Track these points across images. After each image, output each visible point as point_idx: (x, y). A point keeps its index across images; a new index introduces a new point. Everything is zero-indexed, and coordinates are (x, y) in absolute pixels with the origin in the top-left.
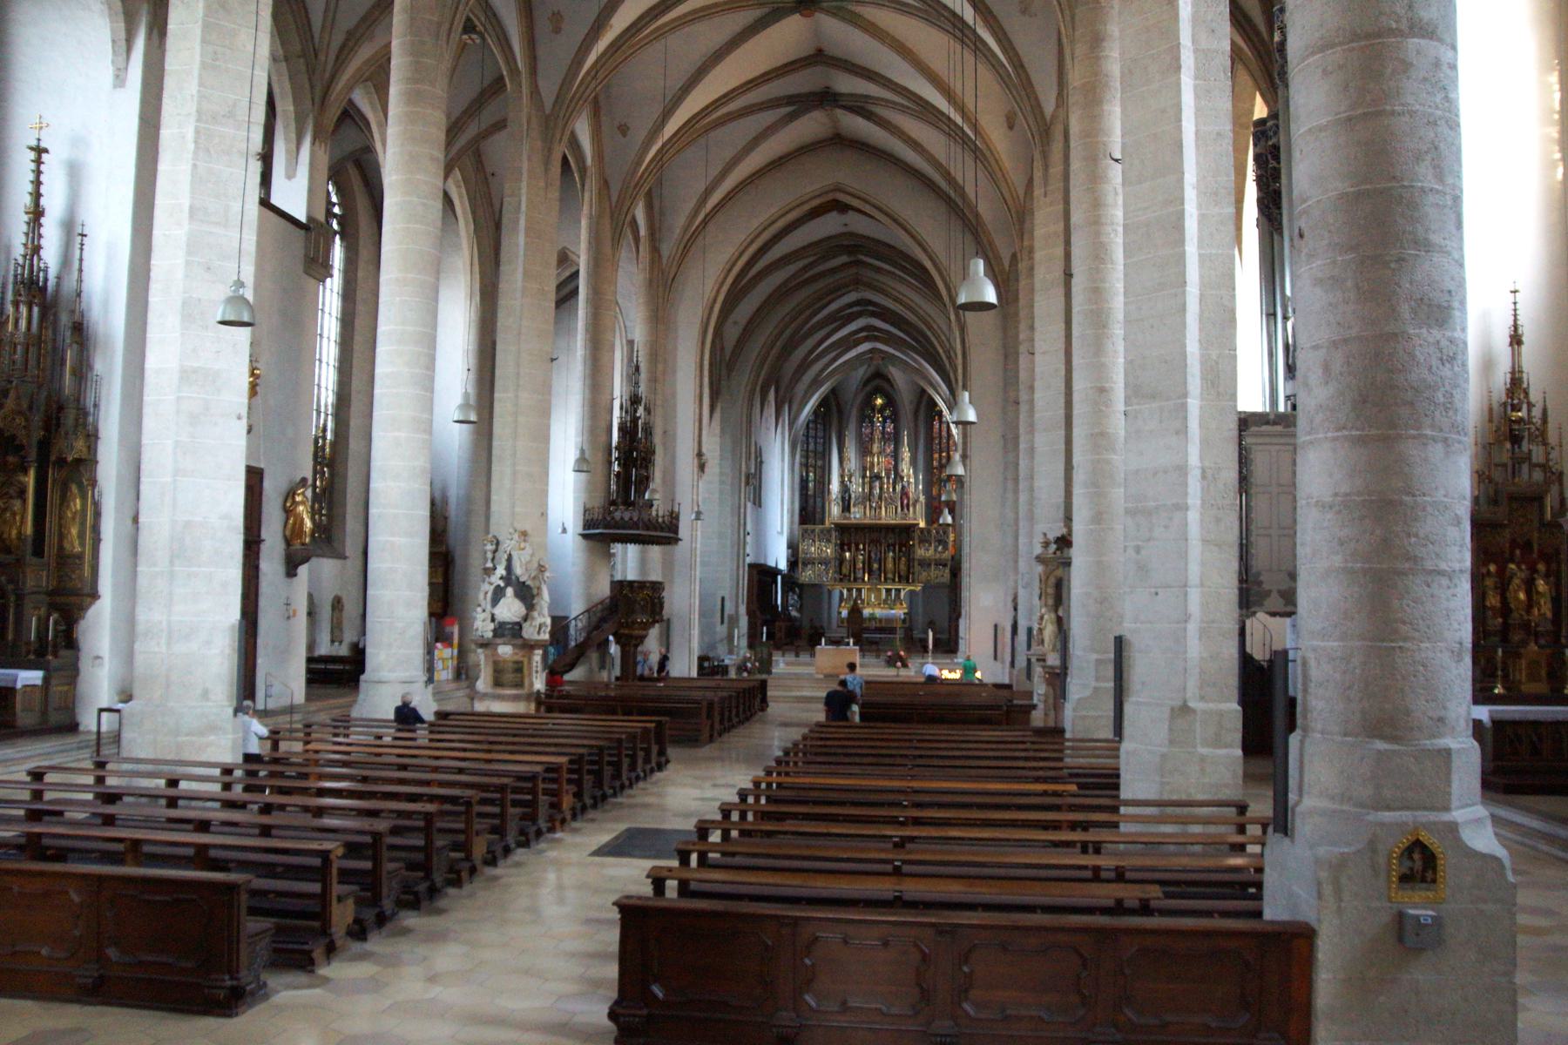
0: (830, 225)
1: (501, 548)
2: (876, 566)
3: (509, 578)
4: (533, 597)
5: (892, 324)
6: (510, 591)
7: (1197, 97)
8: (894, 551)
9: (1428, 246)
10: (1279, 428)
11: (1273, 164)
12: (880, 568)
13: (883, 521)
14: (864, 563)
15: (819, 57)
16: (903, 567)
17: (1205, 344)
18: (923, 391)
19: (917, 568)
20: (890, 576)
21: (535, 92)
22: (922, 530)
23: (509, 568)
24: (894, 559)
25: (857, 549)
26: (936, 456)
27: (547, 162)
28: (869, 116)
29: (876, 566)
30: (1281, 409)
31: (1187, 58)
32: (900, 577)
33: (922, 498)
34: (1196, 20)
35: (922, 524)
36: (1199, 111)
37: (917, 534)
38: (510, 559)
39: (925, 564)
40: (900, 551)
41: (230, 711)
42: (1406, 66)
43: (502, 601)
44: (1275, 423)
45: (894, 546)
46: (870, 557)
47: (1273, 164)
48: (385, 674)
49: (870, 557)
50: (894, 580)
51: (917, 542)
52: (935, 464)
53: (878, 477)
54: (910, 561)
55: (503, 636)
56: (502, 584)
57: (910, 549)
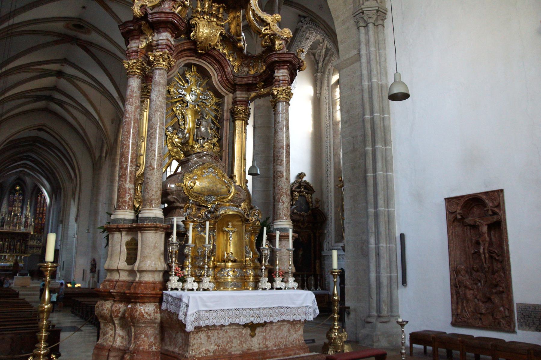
0: (34, 133)
2: (12, 247)
5: (35, 164)
8: (20, 242)
12: (14, 248)
13: (17, 231)
14: (7, 246)
15: (55, 88)
16: (23, 248)
18: (36, 186)
19: (29, 249)
20: (18, 251)
22: (32, 235)
24: (20, 245)
25: (5, 241)
26: (38, 209)
28: (62, 107)
29: (12, 247)
32: (21, 251)
33: (33, 224)
35: (32, 233)
37: (30, 236)
39: (32, 247)
40: (23, 242)
45: (20, 240)
46: (10, 244)
49: (10, 244)
50: (19, 252)
51: (29, 239)
52: (38, 212)
53: (16, 215)
54: (26, 246)
57: (27, 241)
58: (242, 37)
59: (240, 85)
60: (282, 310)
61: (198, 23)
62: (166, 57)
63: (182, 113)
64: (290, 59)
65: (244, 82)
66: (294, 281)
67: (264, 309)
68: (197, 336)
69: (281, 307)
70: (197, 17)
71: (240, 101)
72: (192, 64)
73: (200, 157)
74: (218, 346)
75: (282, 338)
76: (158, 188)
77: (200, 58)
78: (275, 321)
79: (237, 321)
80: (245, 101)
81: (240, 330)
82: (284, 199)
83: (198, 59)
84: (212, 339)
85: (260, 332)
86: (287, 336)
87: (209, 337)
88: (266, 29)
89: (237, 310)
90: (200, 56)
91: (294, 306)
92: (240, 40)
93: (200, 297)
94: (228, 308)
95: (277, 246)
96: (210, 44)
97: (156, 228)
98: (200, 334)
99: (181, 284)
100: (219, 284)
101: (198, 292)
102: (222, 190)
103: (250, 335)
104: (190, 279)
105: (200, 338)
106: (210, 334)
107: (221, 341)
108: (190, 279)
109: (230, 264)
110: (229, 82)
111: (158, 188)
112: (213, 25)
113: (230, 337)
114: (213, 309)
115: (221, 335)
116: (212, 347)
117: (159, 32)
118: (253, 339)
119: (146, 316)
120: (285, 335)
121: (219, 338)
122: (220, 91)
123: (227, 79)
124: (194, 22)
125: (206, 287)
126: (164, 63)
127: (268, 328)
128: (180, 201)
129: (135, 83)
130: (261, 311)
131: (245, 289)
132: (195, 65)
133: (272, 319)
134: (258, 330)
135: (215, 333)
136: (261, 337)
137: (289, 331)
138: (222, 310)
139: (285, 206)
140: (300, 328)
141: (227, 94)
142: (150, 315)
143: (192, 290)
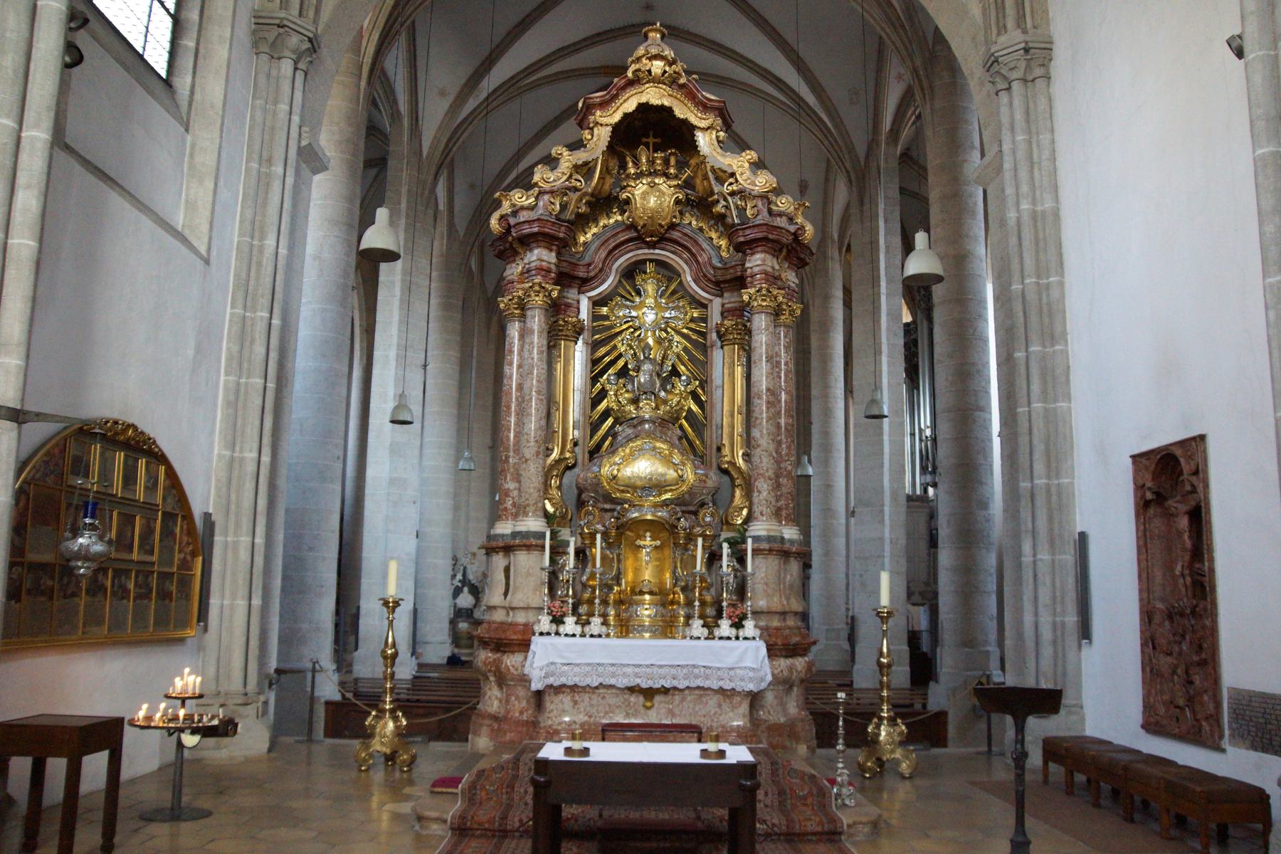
1: (459, 563)
3: (465, 581)
4: (478, 593)
6: (466, 589)
7: (889, 367)
9: (981, 483)
10: (917, 503)
11: (913, 349)
17: (891, 481)
21: (483, 283)
23: (464, 575)
27: (488, 326)
30: (918, 492)
31: (885, 348)
34: (888, 329)
36: (890, 373)
38: (465, 568)
41: (409, 654)
42: (975, 421)
43: (461, 595)
44: (916, 501)
47: (913, 349)
48: (429, 639)
55: (461, 616)
56: (460, 585)
58: (716, 197)
59: (725, 282)
60: (696, 671)
61: (633, 195)
62: (537, 288)
63: (631, 348)
64: (760, 235)
65: (728, 277)
66: (731, 626)
67: (661, 666)
68: (557, 699)
69: (694, 666)
70: (628, 186)
71: (729, 311)
72: (644, 262)
73: (635, 427)
74: (590, 717)
75: (705, 716)
76: (535, 488)
77: (654, 248)
78: (681, 687)
79: (612, 681)
80: (735, 309)
81: (626, 696)
82: (759, 486)
83: (652, 251)
84: (581, 706)
85: (661, 702)
86: (715, 713)
87: (576, 703)
88: (731, 184)
89: (613, 665)
90: (652, 246)
91: (718, 665)
92: (718, 201)
93: (552, 644)
94: (597, 661)
95: (749, 569)
96: (660, 225)
97: (528, 547)
98: (561, 696)
99: (554, 627)
100: (626, 628)
101: (583, 639)
102: (668, 477)
103: (644, 706)
104: (570, 620)
105: (561, 702)
106: (577, 698)
107: (594, 710)
108: (570, 620)
109: (647, 597)
110: (709, 280)
111: (535, 488)
112: (660, 191)
113: (610, 705)
114: (574, 662)
115: (594, 702)
116: (581, 716)
117: (531, 250)
118: (650, 712)
119: (512, 669)
120: (712, 712)
121: (591, 705)
122: (697, 297)
123: (705, 276)
124: (624, 196)
125: (596, 633)
126: (537, 299)
127: (677, 698)
128: (601, 499)
129: (514, 330)
130: (655, 669)
131: (672, 638)
132: (651, 261)
133: (675, 683)
134: (658, 698)
135: (586, 697)
136: (664, 710)
137: (720, 706)
138: (589, 664)
139: (761, 497)
140: (740, 703)
141: (711, 301)
142: (517, 670)
143: (574, 635)
